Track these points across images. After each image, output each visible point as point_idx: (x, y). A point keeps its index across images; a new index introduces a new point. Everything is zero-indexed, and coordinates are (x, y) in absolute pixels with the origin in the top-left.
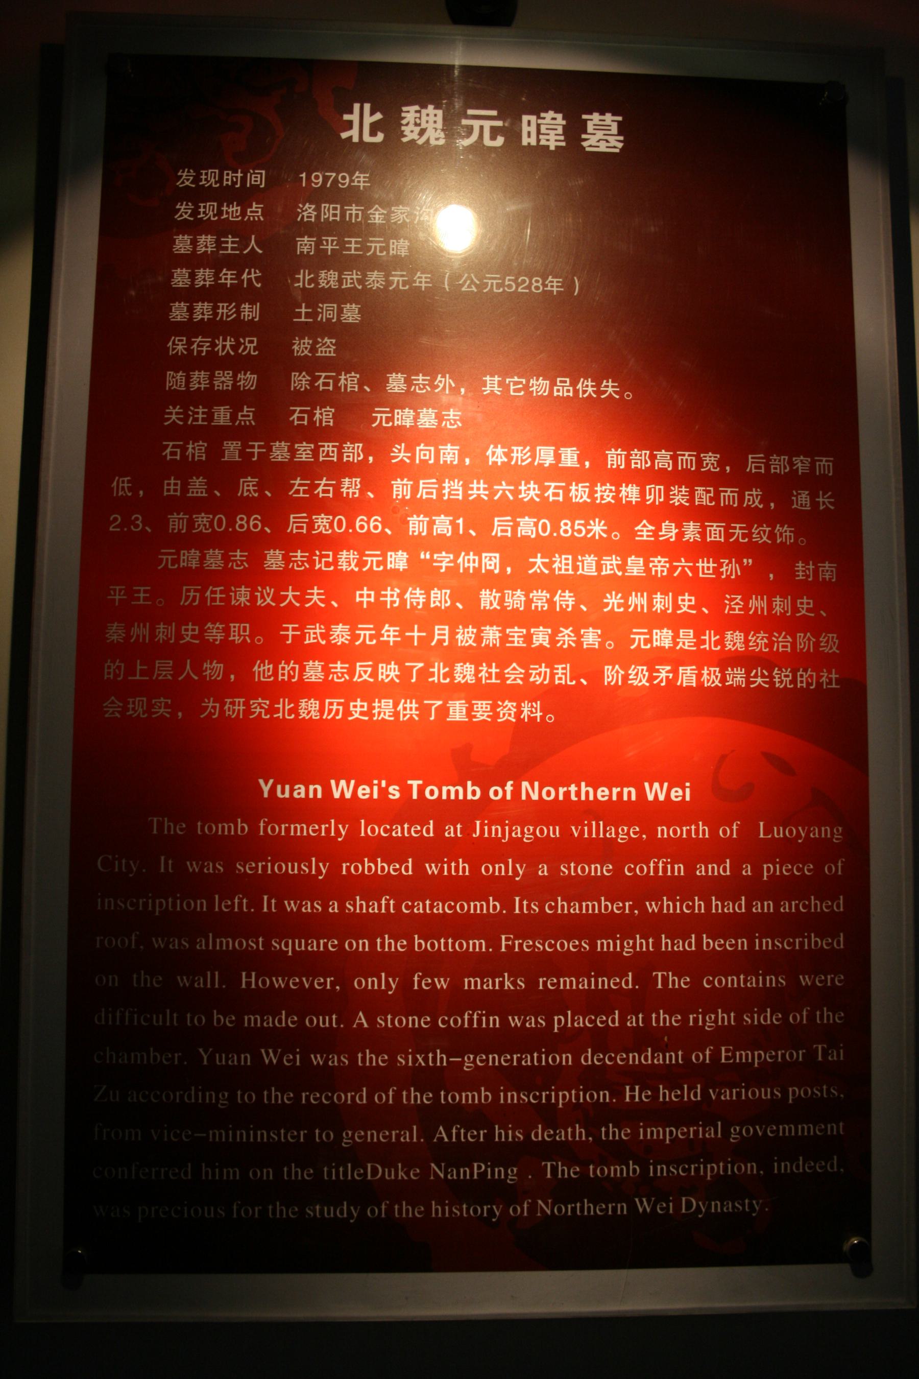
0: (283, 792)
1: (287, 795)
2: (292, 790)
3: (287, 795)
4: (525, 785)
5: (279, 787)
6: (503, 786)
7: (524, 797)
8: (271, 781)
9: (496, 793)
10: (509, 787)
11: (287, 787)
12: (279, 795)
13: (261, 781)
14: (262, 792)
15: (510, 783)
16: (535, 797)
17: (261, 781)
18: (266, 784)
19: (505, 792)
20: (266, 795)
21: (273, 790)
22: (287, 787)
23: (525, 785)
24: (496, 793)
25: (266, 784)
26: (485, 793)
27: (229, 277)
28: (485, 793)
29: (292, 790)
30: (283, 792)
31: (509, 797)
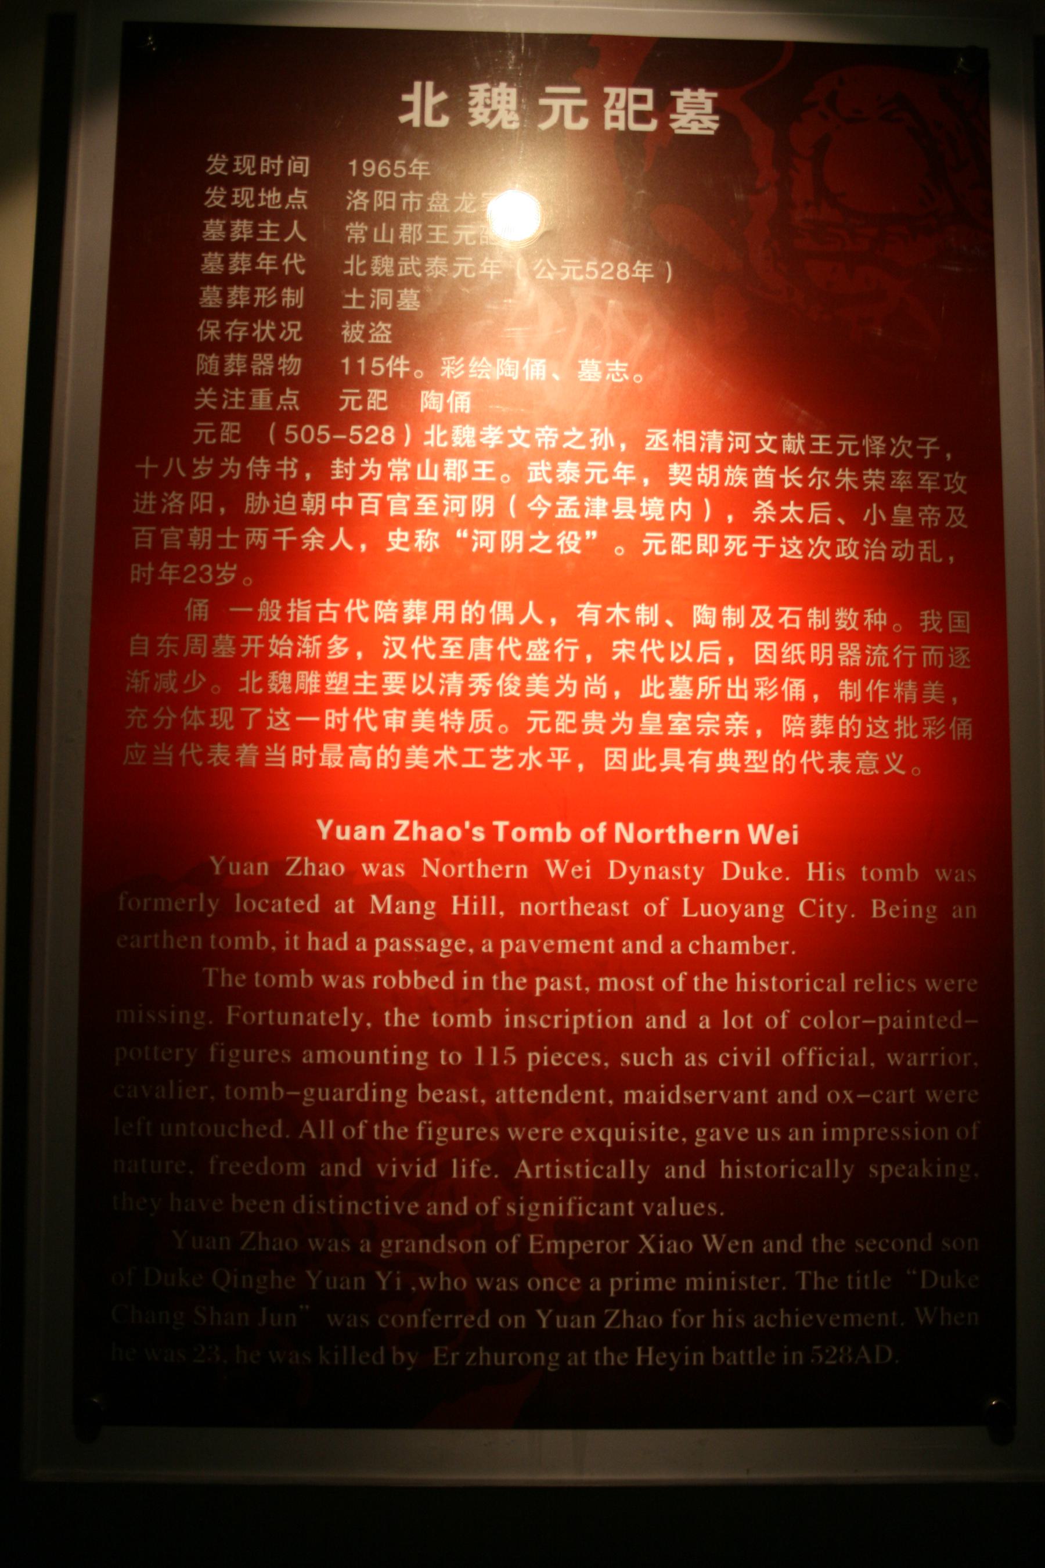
0: (343, 833)
1: (347, 837)
2: (353, 832)
3: (347, 837)
4: (619, 826)
5: (339, 828)
6: (595, 827)
7: (617, 840)
8: (330, 822)
9: (588, 835)
10: (602, 828)
11: (348, 828)
12: (339, 836)
13: (320, 822)
14: (320, 833)
15: (603, 824)
16: (630, 839)
17: (320, 822)
18: (325, 823)
19: (597, 834)
20: (325, 837)
21: (332, 830)
22: (348, 828)
23: (619, 826)
24: (588, 835)
25: (325, 823)
26: (576, 835)
27: (268, 262)
28: (576, 835)
29: (353, 832)
30: (343, 833)
31: (601, 839)
